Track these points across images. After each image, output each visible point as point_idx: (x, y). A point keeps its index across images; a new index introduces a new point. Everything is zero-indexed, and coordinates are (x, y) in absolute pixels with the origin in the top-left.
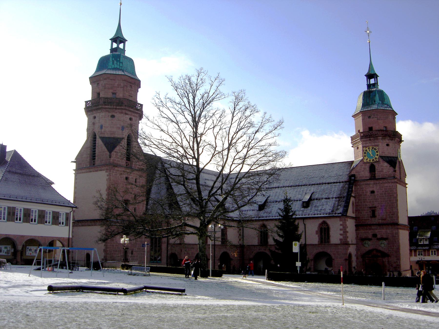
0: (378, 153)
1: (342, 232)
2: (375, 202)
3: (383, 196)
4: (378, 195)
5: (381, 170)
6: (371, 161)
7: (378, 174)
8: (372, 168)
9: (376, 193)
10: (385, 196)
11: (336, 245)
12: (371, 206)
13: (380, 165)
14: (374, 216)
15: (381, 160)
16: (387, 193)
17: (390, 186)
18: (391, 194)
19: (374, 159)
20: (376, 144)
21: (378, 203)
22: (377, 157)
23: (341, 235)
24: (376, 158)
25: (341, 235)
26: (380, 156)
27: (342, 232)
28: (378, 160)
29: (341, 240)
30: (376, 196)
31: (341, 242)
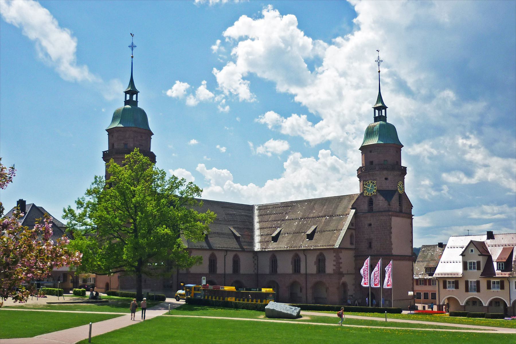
0: (376, 187)
1: (335, 263)
7: (375, 208)
8: (371, 202)
9: (373, 226)
11: (330, 275)
14: (370, 247)
19: (372, 192)
20: (374, 178)
22: (375, 191)
23: (334, 265)
24: (374, 192)
25: (334, 265)
26: (377, 190)
27: (335, 263)
28: (375, 194)
29: (334, 270)
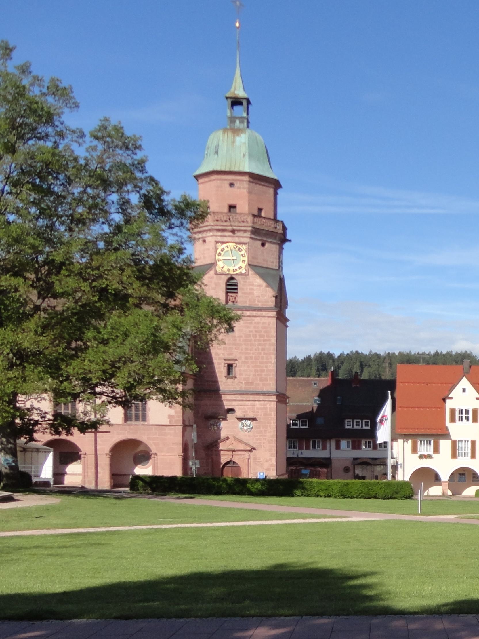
2: (235, 349)
3: (251, 340)
4: (241, 337)
5: (248, 291)
6: (231, 272)
10: (255, 341)
12: (226, 357)
13: (248, 281)
15: (251, 272)
16: (258, 334)
17: (264, 323)
18: (266, 338)
21: (240, 353)
29: (170, 416)
30: (238, 339)
31: (170, 421)
